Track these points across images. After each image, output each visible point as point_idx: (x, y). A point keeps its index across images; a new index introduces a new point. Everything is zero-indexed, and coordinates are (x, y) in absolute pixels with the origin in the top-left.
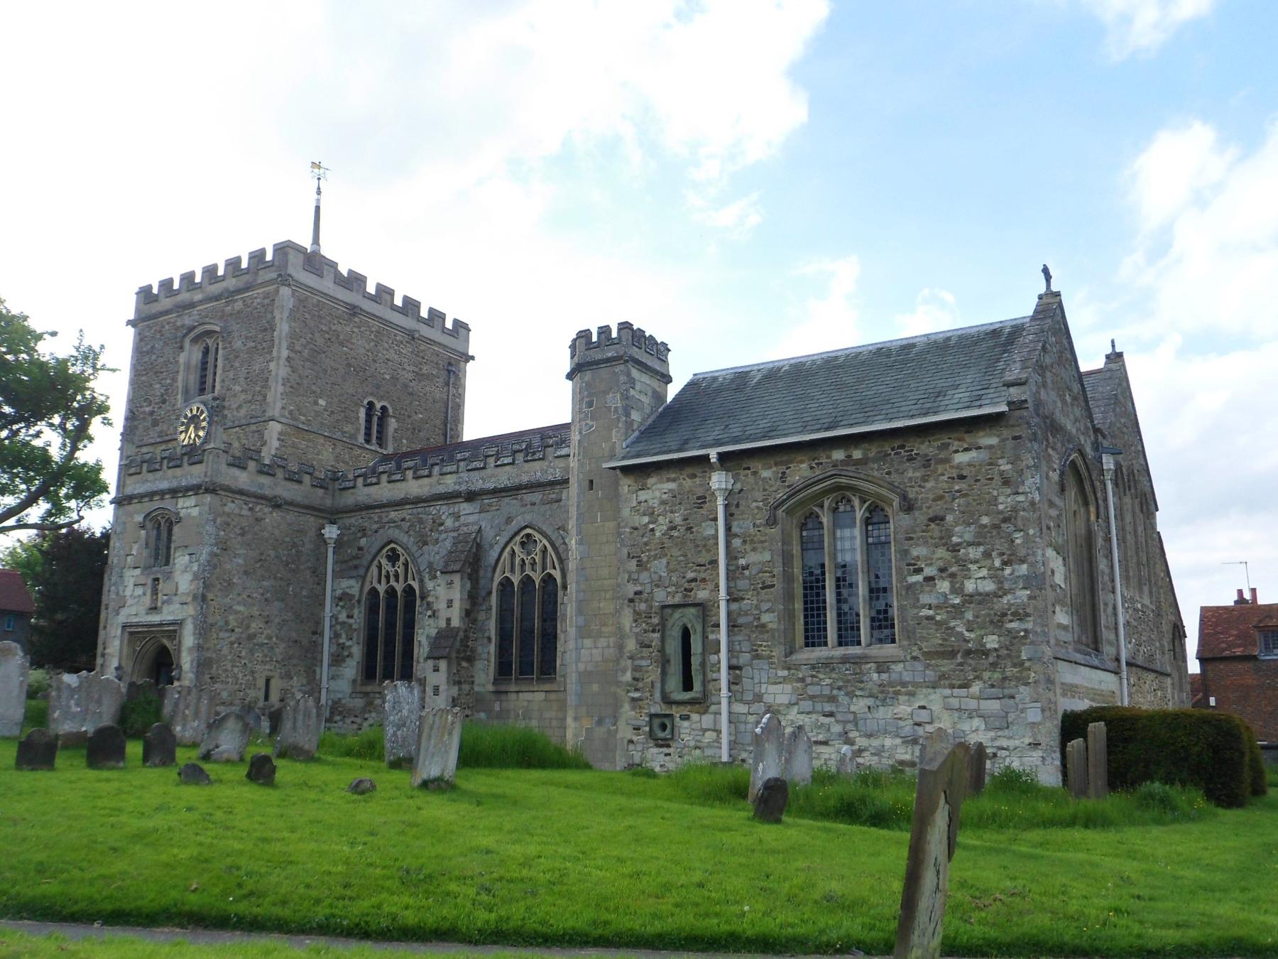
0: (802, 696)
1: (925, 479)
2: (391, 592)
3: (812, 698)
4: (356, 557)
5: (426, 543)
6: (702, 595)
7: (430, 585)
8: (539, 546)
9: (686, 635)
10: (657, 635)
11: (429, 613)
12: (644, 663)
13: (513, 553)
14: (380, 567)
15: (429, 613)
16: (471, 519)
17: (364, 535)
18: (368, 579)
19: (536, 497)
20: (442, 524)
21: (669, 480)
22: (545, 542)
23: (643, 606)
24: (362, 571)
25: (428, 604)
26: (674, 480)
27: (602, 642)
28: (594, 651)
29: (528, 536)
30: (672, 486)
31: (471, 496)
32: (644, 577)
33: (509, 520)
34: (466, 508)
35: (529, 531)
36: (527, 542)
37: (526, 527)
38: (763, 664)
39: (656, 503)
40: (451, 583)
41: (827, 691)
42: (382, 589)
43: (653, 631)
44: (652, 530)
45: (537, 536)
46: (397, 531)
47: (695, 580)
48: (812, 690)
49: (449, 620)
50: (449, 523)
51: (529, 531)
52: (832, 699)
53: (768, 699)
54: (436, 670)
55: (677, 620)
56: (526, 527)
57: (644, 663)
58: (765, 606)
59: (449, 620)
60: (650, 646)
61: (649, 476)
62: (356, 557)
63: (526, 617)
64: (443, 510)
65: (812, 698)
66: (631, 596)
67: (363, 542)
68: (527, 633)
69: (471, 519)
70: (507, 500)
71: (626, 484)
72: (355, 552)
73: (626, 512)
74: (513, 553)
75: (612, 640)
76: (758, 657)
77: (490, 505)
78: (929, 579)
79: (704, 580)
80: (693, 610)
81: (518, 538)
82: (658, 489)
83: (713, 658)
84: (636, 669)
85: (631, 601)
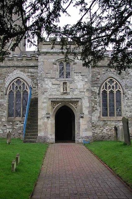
2: (112, 92)
4: (96, 81)
5: (124, 79)
7: (125, 91)
11: (126, 98)
14: (106, 84)
15: (126, 98)
17: (99, 75)
18: (102, 87)
20: (129, 74)
24: (100, 85)
25: (126, 96)
42: (115, 91)
46: (112, 75)
62: (96, 81)
67: (99, 76)
72: (96, 79)
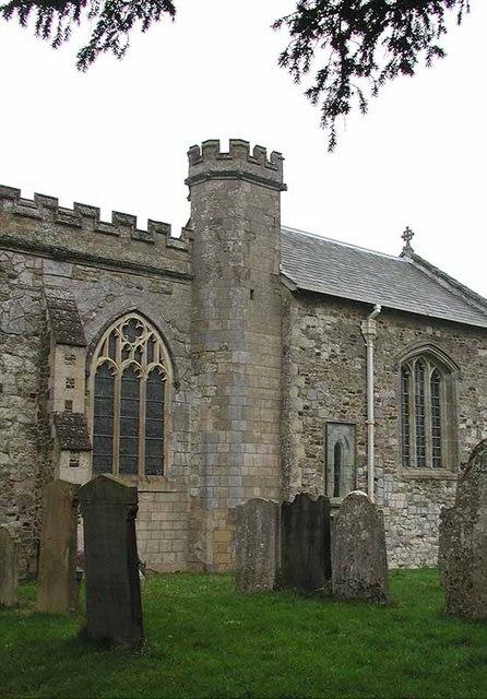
0: (410, 501)
1: (468, 360)
3: (416, 504)
6: (354, 415)
8: (146, 336)
9: (338, 447)
10: (320, 447)
12: (309, 471)
13: (114, 337)
16: (59, 282)
19: (145, 281)
20: (14, 277)
21: (331, 314)
22: (154, 332)
23: (310, 420)
26: (335, 315)
27: (262, 448)
28: (255, 456)
29: (134, 321)
30: (334, 320)
31: (60, 256)
32: (311, 393)
33: (110, 297)
34: (50, 266)
35: (136, 316)
36: (133, 329)
37: (131, 312)
38: (389, 477)
39: (320, 330)
40: (72, 358)
41: (423, 499)
43: (318, 443)
44: (318, 354)
45: (146, 324)
47: (347, 404)
48: (417, 498)
49: (69, 404)
50: (26, 278)
51: (136, 316)
52: (425, 505)
53: (392, 504)
54: (74, 464)
55: (338, 434)
56: (131, 312)
57: (309, 471)
58: (392, 433)
59: (69, 404)
60: (314, 457)
61: (316, 305)
63: (131, 413)
64: (20, 261)
65: (416, 504)
66: (301, 410)
68: (130, 429)
69: (59, 282)
70: (107, 274)
71: (296, 309)
73: (296, 332)
74: (114, 337)
75: (272, 447)
76: (387, 472)
77: (86, 273)
78: (469, 427)
79: (353, 405)
80: (346, 429)
81: (122, 322)
82: (323, 320)
83: (360, 470)
84: (305, 476)
85: (301, 414)
